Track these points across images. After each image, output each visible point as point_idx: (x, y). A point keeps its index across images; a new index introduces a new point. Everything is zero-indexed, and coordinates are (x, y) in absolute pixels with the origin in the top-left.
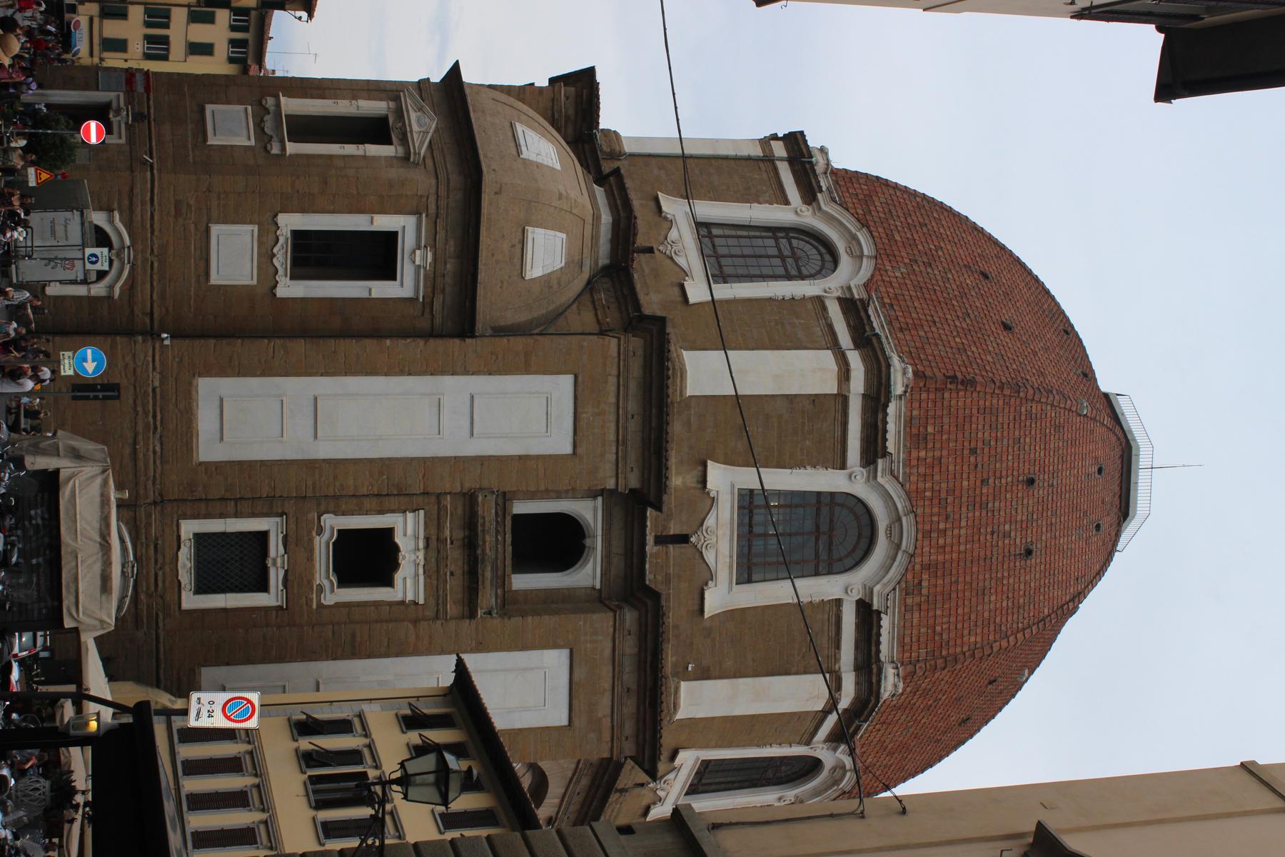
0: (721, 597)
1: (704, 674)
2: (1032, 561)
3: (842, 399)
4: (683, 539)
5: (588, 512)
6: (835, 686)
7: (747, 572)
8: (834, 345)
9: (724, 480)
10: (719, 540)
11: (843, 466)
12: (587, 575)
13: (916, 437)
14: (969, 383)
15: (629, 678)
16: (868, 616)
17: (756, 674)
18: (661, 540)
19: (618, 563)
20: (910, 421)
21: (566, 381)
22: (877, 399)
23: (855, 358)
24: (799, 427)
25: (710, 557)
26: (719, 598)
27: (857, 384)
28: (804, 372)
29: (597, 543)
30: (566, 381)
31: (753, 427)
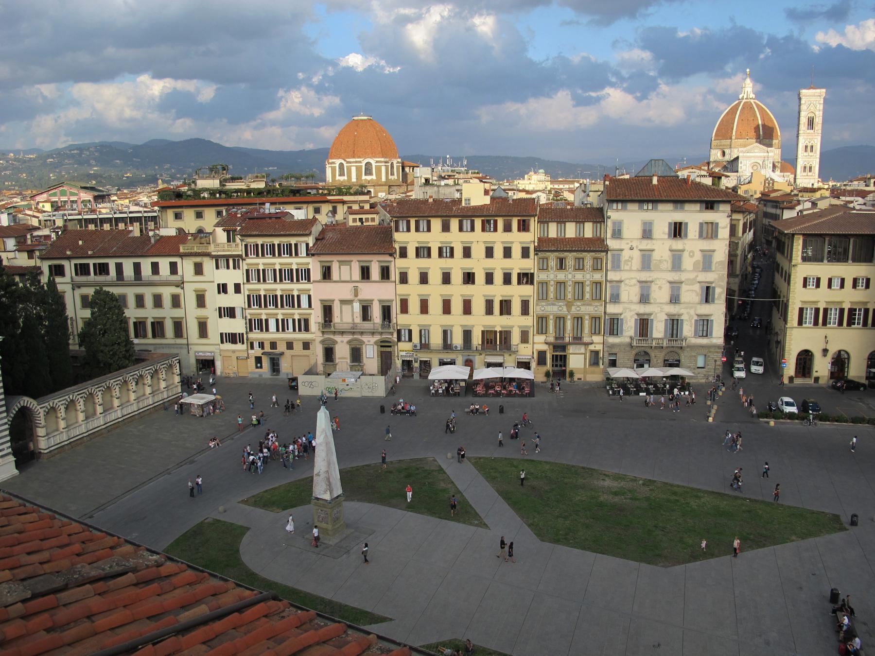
0: (374, 177)
9: (364, 177)
12: (372, 190)
13: (359, 157)
16: (377, 162)
22: (356, 162)
24: (358, 169)
26: (374, 177)
28: (354, 170)
31: (359, 176)
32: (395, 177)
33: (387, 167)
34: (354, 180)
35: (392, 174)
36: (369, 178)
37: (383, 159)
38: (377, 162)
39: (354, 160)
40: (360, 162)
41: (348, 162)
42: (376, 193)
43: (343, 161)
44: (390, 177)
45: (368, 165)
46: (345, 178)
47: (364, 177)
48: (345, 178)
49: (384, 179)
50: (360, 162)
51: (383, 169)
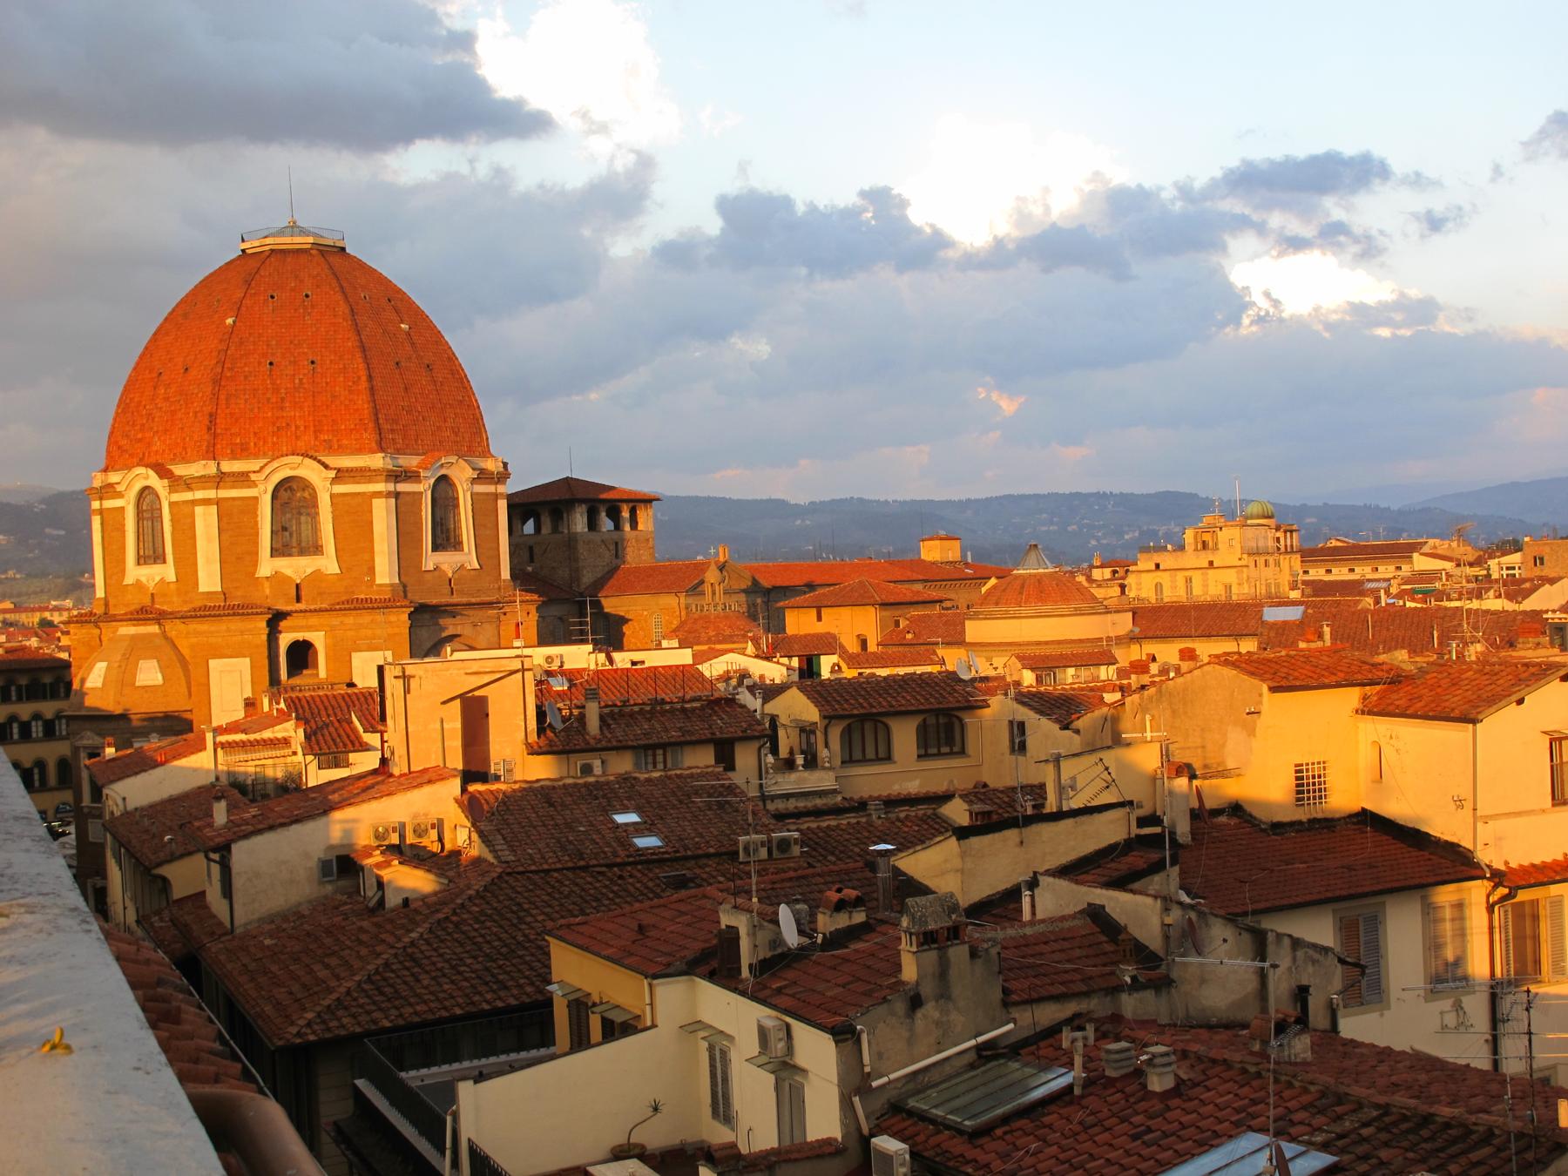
0: (328, 563)
1: (372, 570)
2: (317, 359)
3: (218, 502)
4: (298, 586)
5: (285, 640)
6: (378, 494)
7: (317, 549)
8: (194, 503)
9: (267, 566)
10: (296, 567)
11: (256, 499)
12: (318, 639)
13: (241, 452)
14: (212, 417)
15: (366, 618)
16: (342, 475)
17: (372, 541)
18: (298, 599)
19: (314, 620)
20: (234, 457)
21: (212, 663)
22: (220, 479)
23: (199, 495)
24: (235, 521)
25: (309, 571)
26: (328, 563)
27: (211, 494)
28: (206, 523)
29: (300, 636)
30: (212, 663)
31: (236, 553)
32: (468, 557)
33: (404, 509)
34: (209, 579)
35: (445, 539)
36: (296, 567)
37: (377, 461)
38: (342, 475)
39: (207, 468)
40: (243, 479)
41: (177, 483)
42: (341, 657)
43: (154, 480)
44: (430, 560)
45: (290, 495)
46: (167, 571)
47: (267, 566)
48: (167, 571)
49: (385, 572)
50: (243, 479)
51: (382, 517)
